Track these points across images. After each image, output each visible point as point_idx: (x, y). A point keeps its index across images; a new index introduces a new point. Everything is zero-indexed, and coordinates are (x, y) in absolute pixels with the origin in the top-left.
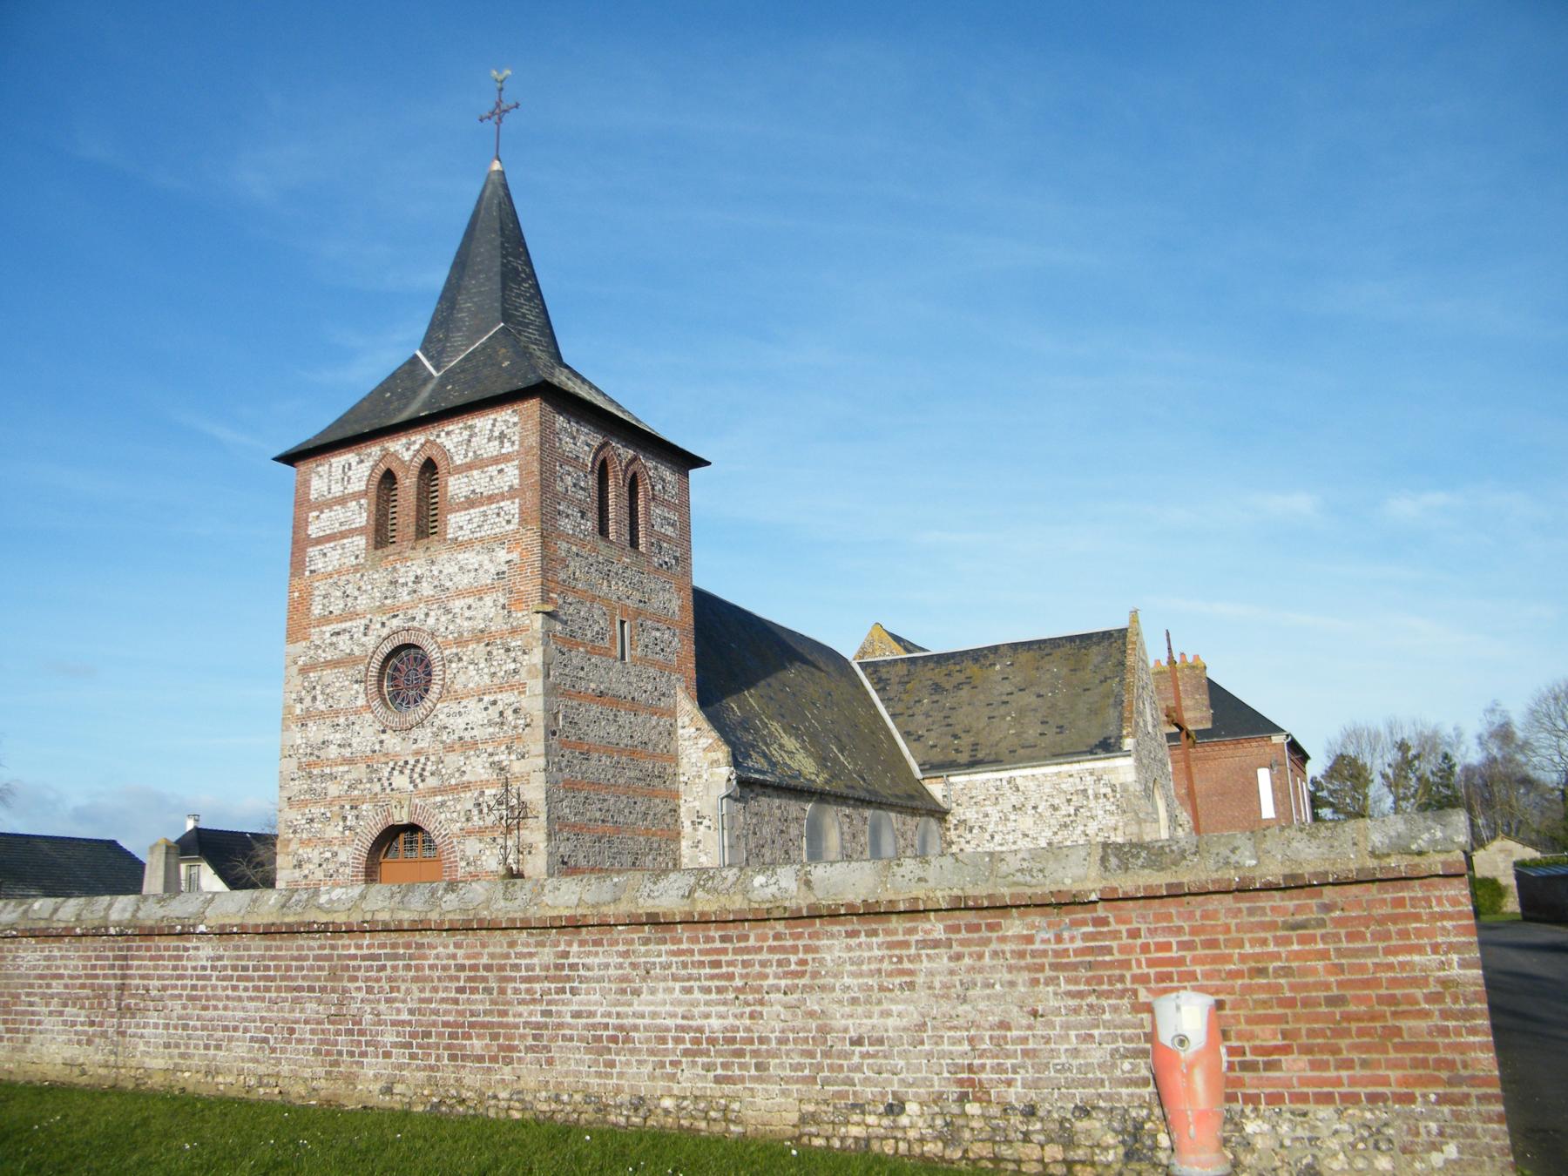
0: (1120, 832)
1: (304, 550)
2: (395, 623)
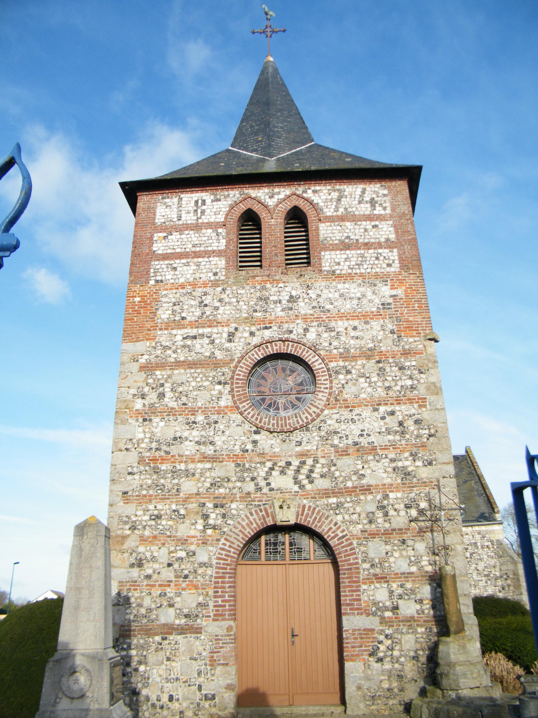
0: (497, 569)
1: (148, 263)
2: (267, 334)
